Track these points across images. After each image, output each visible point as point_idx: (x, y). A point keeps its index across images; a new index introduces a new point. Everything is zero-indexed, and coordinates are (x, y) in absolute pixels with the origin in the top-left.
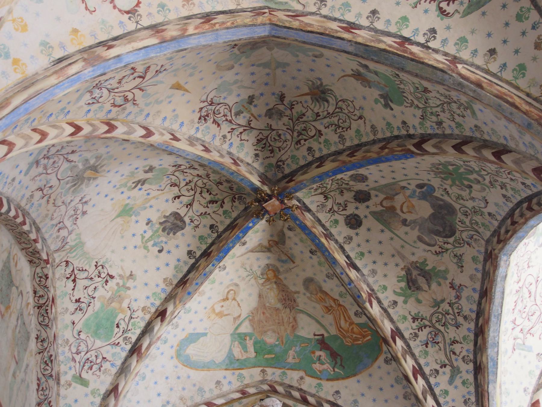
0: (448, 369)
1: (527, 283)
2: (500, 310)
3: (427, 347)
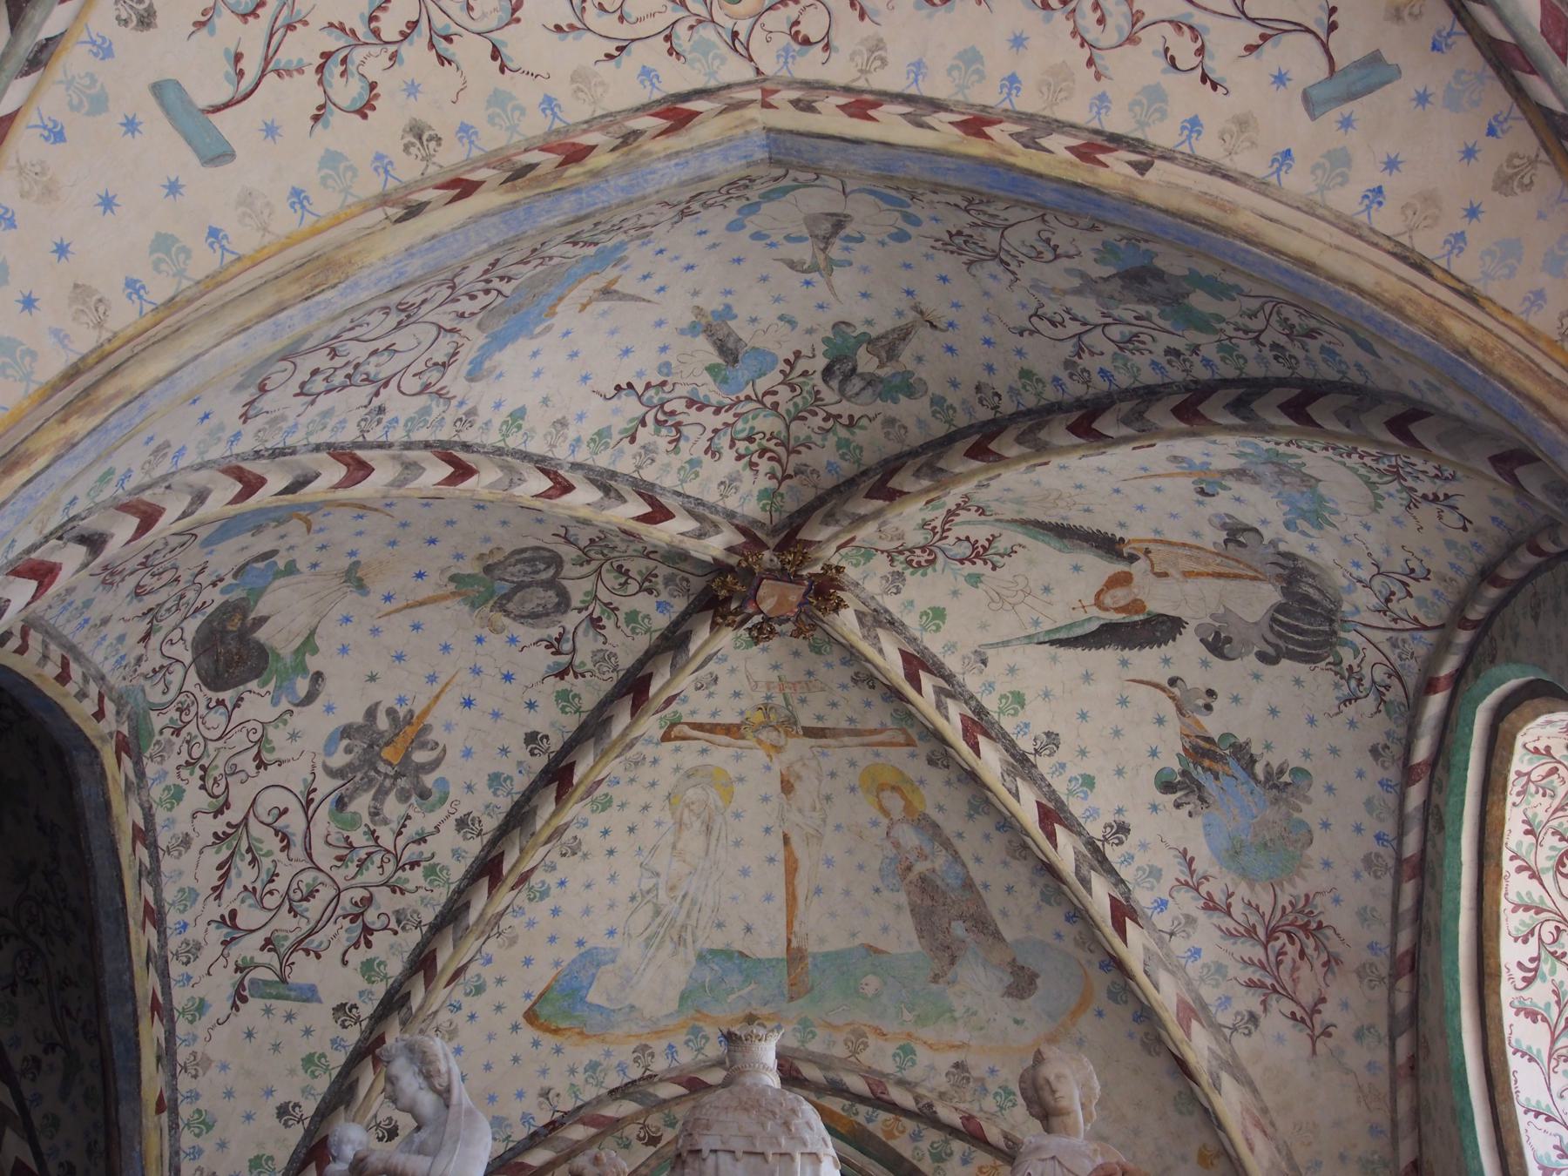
1: (261, 809)
2: (118, 898)
3: (14, 993)
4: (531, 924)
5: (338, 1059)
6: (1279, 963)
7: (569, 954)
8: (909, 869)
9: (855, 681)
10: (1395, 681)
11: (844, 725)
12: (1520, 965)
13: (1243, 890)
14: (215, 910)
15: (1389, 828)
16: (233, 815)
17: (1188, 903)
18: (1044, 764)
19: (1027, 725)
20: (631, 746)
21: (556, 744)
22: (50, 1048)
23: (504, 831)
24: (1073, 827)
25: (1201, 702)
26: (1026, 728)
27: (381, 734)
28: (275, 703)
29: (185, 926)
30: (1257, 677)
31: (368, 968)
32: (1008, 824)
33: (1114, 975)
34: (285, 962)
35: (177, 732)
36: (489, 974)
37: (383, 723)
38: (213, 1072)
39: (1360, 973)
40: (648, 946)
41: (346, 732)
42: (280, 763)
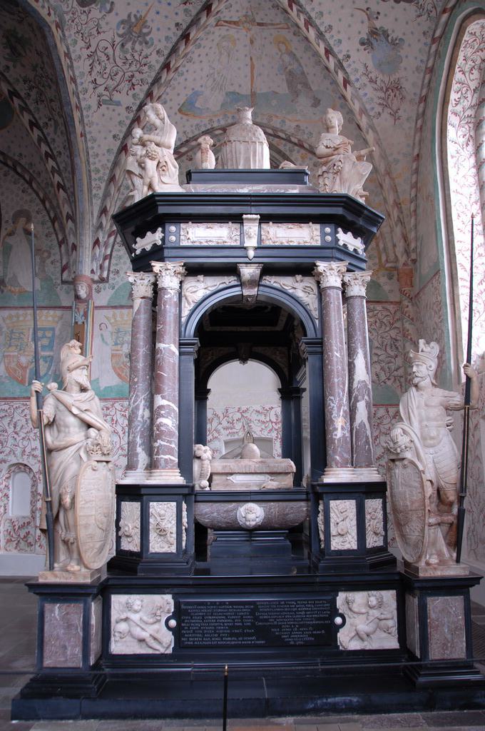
0: (52, 122)
4: (179, 83)
5: (128, 122)
6: (388, 98)
7: (190, 92)
8: (286, 68)
9: (273, 7)
10: (434, 10)
11: (269, 22)
12: (455, 100)
13: (381, 77)
14: (90, 79)
15: (425, 58)
16: (92, 49)
17: (365, 80)
18: (327, 36)
19: (323, 23)
20: (206, 27)
21: (184, 27)
22: (50, 120)
23: (170, 55)
24: (335, 56)
25: (375, 16)
26: (322, 23)
27: (133, 23)
28: (100, 12)
29: (82, 83)
30: (393, 8)
31: (134, 96)
32: (316, 54)
33: (343, 100)
34: (111, 94)
35: (73, 21)
36: (168, 98)
37: (133, 19)
38: (95, 126)
39: (411, 101)
40: (212, 90)
41: (123, 22)
42: (104, 32)
